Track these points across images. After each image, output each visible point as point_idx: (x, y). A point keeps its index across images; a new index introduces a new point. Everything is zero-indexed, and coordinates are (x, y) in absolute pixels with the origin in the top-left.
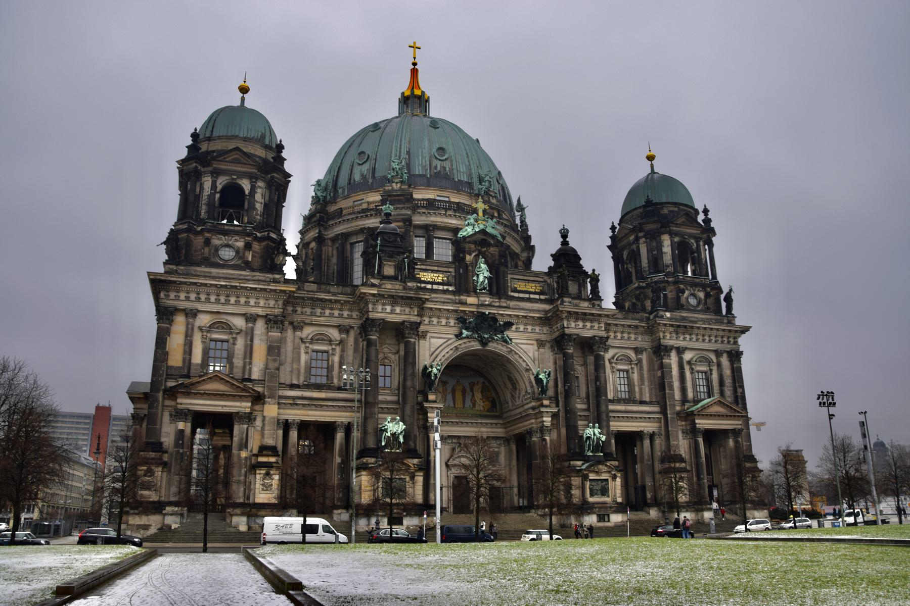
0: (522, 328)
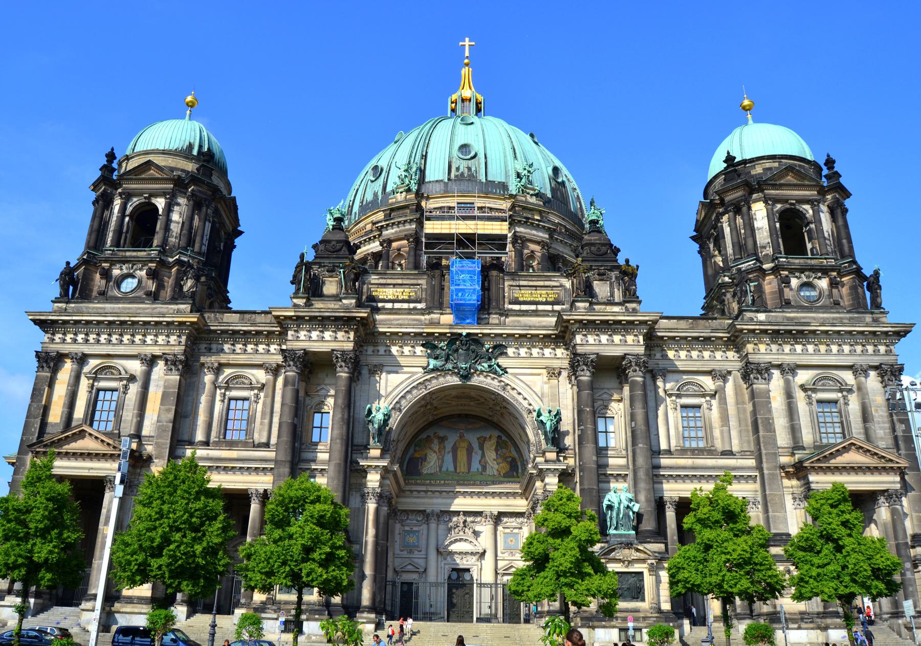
0: (523, 351)
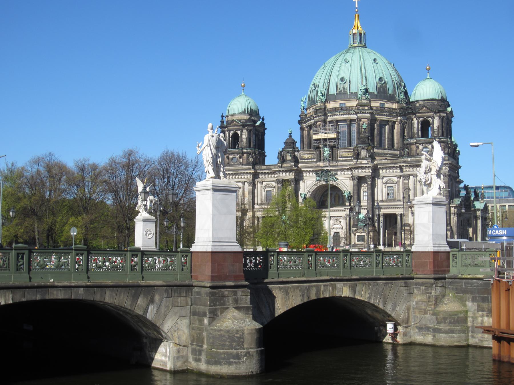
0: (342, 173)
